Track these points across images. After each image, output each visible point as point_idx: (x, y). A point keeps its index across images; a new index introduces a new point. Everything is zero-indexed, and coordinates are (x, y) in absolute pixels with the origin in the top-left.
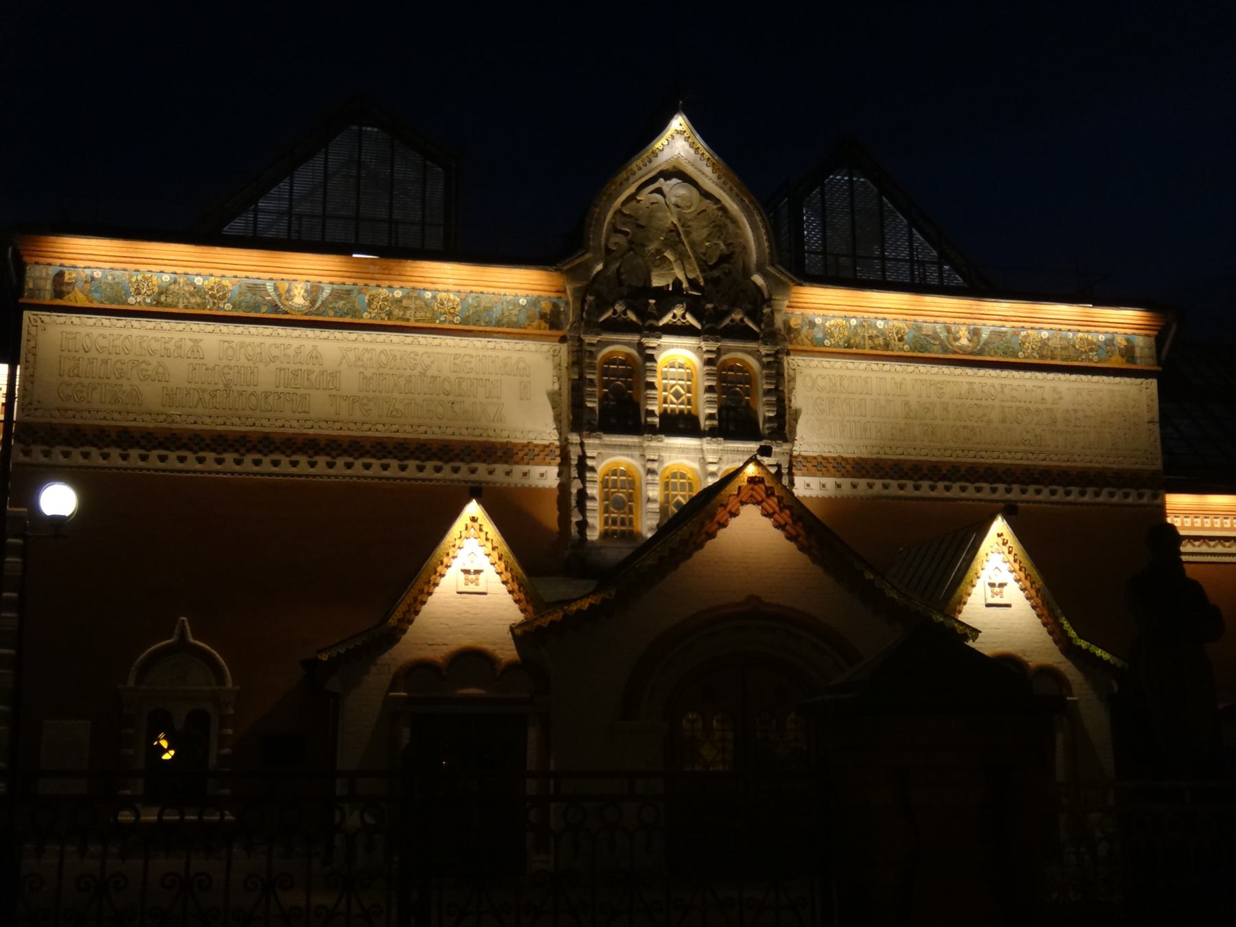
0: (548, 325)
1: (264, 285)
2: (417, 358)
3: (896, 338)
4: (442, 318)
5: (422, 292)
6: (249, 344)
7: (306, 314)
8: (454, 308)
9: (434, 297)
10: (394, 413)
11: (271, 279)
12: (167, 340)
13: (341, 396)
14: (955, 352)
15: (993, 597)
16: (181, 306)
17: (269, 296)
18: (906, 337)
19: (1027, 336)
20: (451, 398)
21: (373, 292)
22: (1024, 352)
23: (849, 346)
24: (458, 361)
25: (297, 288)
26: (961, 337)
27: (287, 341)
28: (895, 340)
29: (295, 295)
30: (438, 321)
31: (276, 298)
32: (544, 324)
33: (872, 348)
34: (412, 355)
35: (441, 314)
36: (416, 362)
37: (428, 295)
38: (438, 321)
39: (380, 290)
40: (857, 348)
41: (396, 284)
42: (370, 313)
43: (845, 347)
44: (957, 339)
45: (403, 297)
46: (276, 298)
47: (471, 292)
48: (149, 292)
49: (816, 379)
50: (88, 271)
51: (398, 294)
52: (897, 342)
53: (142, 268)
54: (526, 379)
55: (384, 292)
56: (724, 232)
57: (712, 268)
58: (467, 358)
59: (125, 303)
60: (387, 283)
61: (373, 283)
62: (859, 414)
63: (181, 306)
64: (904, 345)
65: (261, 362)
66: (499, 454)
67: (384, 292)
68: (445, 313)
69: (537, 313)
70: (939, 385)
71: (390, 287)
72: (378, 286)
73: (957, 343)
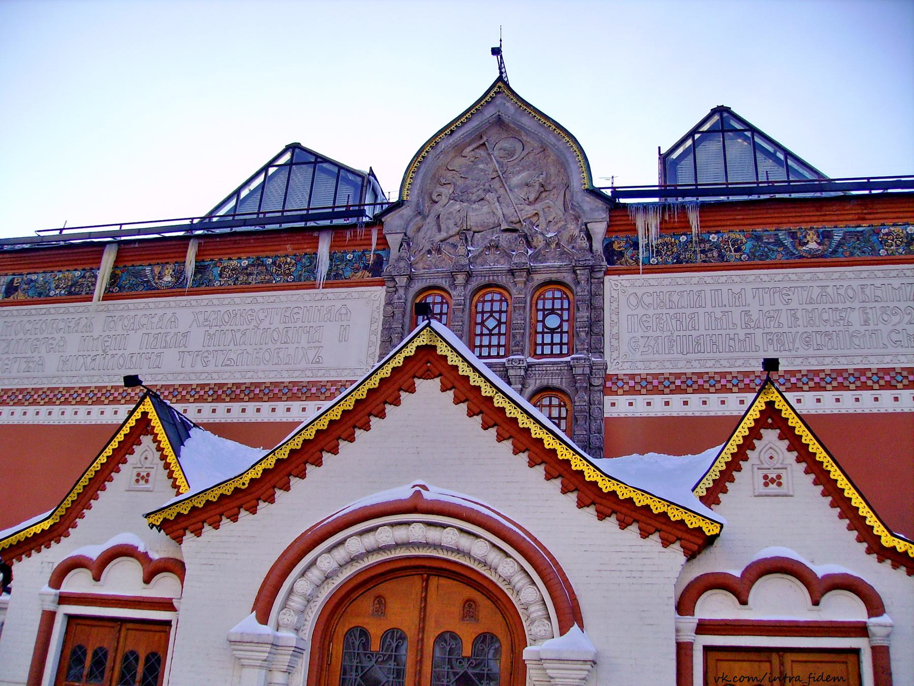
0: (370, 275)
1: (145, 270)
2: (254, 314)
3: (732, 249)
4: (278, 279)
5: (265, 259)
6: (126, 317)
7: (172, 288)
8: (289, 269)
9: (274, 263)
10: (229, 362)
11: (150, 265)
12: (70, 320)
13: (189, 352)
14: (801, 257)
15: (766, 485)
16: (84, 293)
17: (146, 276)
18: (743, 247)
19: (887, 234)
20: (278, 345)
21: (225, 264)
22: (887, 250)
23: (679, 261)
24: (288, 314)
25: (167, 269)
26: (808, 241)
27: (153, 312)
28: (731, 252)
29: (165, 274)
30: (274, 282)
31: (151, 279)
32: (367, 274)
33: (704, 261)
34: (250, 312)
35: (278, 275)
36: (252, 318)
37: (269, 261)
38: (274, 282)
39: (231, 262)
40: (687, 262)
41: (243, 256)
42: (220, 281)
43: (673, 263)
44: (807, 243)
45: (248, 266)
46: (151, 279)
47: (306, 254)
48: (64, 286)
49: (642, 297)
50: (29, 276)
51: (245, 263)
52: (733, 253)
53: (64, 269)
54: (345, 323)
55: (234, 263)
56: (544, 173)
57: (530, 204)
58: (296, 310)
59: (48, 296)
60: (238, 255)
61: (225, 258)
62: (690, 328)
63: (84, 293)
64: (741, 255)
65: (133, 329)
66: (314, 390)
67: (234, 263)
68: (280, 275)
69: (362, 266)
70: (784, 292)
71: (239, 258)
72: (230, 259)
73: (804, 248)
